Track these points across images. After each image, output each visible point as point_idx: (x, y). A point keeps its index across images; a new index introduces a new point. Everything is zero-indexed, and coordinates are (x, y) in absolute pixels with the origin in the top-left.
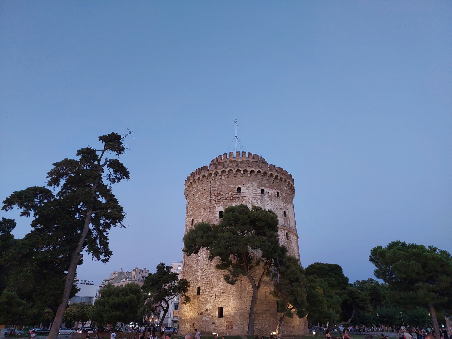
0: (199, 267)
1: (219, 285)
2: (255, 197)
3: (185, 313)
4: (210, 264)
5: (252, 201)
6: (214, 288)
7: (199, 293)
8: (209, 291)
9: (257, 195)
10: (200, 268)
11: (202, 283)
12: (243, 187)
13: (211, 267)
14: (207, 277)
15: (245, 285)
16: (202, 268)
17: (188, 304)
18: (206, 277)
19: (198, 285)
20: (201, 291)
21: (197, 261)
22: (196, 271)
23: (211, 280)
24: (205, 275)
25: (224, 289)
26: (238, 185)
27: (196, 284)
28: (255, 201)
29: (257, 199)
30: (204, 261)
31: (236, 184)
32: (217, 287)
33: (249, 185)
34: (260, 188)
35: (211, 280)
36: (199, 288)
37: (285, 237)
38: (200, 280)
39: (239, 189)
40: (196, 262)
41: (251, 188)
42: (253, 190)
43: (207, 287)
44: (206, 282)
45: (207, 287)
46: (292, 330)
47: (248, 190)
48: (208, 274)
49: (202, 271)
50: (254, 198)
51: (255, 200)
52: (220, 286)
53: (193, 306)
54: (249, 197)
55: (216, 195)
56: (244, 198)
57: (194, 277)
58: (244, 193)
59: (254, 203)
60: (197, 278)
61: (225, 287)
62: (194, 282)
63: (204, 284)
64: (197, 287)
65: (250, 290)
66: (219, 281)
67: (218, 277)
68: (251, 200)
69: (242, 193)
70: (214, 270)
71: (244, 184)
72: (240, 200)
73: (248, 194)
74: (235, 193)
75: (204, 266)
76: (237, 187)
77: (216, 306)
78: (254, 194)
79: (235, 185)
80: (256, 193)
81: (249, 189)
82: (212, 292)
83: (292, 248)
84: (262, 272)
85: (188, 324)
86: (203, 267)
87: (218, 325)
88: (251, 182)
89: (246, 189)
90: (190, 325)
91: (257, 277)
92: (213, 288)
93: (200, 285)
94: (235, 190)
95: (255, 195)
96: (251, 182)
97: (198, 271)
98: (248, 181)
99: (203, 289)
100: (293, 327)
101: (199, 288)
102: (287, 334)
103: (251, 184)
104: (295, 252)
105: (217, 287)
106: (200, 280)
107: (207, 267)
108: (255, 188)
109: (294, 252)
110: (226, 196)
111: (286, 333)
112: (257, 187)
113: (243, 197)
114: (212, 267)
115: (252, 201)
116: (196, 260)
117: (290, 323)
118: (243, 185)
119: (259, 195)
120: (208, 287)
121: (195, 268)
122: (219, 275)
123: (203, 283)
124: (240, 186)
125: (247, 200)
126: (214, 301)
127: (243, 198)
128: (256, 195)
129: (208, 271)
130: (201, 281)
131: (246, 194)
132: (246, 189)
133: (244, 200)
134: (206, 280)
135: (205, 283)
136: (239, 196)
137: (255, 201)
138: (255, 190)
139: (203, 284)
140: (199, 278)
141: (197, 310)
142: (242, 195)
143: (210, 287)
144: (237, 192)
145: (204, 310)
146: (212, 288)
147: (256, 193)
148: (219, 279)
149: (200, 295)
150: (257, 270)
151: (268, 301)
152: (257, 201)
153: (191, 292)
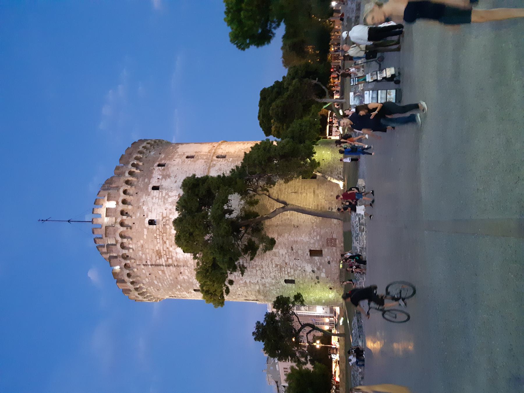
0: (259, 281)
1: (282, 255)
2: (165, 200)
3: (317, 299)
4: (255, 266)
5: (170, 204)
6: (287, 261)
7: (292, 282)
8: (290, 268)
9: (160, 195)
10: (261, 280)
11: (280, 277)
12: (147, 216)
13: (259, 265)
14: (273, 270)
15: (283, 219)
16: (261, 277)
17: (305, 296)
18: (272, 272)
19: (282, 282)
20: (290, 278)
21: (252, 284)
22: (264, 285)
23: (277, 266)
24: (270, 274)
25: (288, 248)
26: (144, 224)
27: (281, 286)
28: (170, 200)
29: (167, 197)
30: (252, 274)
31: (143, 226)
32: (285, 258)
33: (145, 208)
34: (151, 192)
35: (277, 265)
36: (286, 281)
37: (222, 160)
38: (276, 280)
39: (152, 222)
40: (253, 285)
41: (150, 205)
42: (152, 202)
43: (285, 271)
44: (279, 271)
45: (285, 271)
46: (338, 162)
47: (153, 211)
48: (269, 269)
49: (265, 278)
50: (165, 201)
51: (169, 199)
52: (284, 253)
53: (308, 289)
54: (163, 208)
55: (159, 257)
56: (164, 216)
57: (272, 288)
58: (157, 216)
59: (172, 202)
60: (274, 284)
61: (285, 246)
62: (279, 288)
63: (282, 275)
64: (285, 284)
65: (289, 214)
66: (277, 255)
67: (273, 255)
68: (167, 205)
69: (158, 218)
70: (263, 261)
71: (144, 216)
72: (168, 222)
73: (159, 210)
74: (156, 228)
75: (258, 274)
76: (147, 226)
77: (308, 259)
78: (160, 200)
79: (144, 229)
80: (159, 197)
81: (152, 208)
82: (291, 264)
83: (237, 152)
84: (267, 197)
85: (329, 295)
86: (260, 276)
87: (331, 257)
88: (140, 204)
89: (151, 212)
90: (331, 292)
91: (273, 203)
92: (286, 262)
93: (282, 280)
94: (152, 229)
95: (161, 199)
96: (140, 204)
97: (264, 282)
98: (138, 208)
99: (288, 276)
100: (334, 160)
101: (286, 281)
102: (342, 167)
103: (143, 204)
104: (243, 148)
105: (285, 258)
106: (276, 280)
107: (260, 270)
108: (150, 199)
109: (242, 149)
110: (160, 243)
111: (341, 169)
112: (149, 195)
113: (163, 218)
114: (260, 263)
115: (170, 204)
116: (250, 285)
117: (329, 163)
118: (145, 216)
119: (161, 193)
120: (285, 269)
121: (261, 286)
122: (270, 255)
123: (279, 275)
124: (145, 222)
125: (168, 211)
126: (303, 262)
127: (165, 217)
128: (160, 198)
129: (264, 269)
130: (277, 279)
131: (158, 212)
132: (151, 212)
133: (168, 215)
134: (277, 272)
135: (280, 273)
136: (161, 223)
137: (170, 200)
138: (153, 199)
139: (281, 275)
140: (274, 281)
141: (313, 284)
142: (161, 218)
143: (286, 266)
144: (155, 226)
145: (314, 276)
146: (286, 263)
147: (159, 197)
148: (275, 255)
149: (294, 280)
150: (265, 203)
151: (303, 190)
152: (169, 197)
153: (290, 292)
